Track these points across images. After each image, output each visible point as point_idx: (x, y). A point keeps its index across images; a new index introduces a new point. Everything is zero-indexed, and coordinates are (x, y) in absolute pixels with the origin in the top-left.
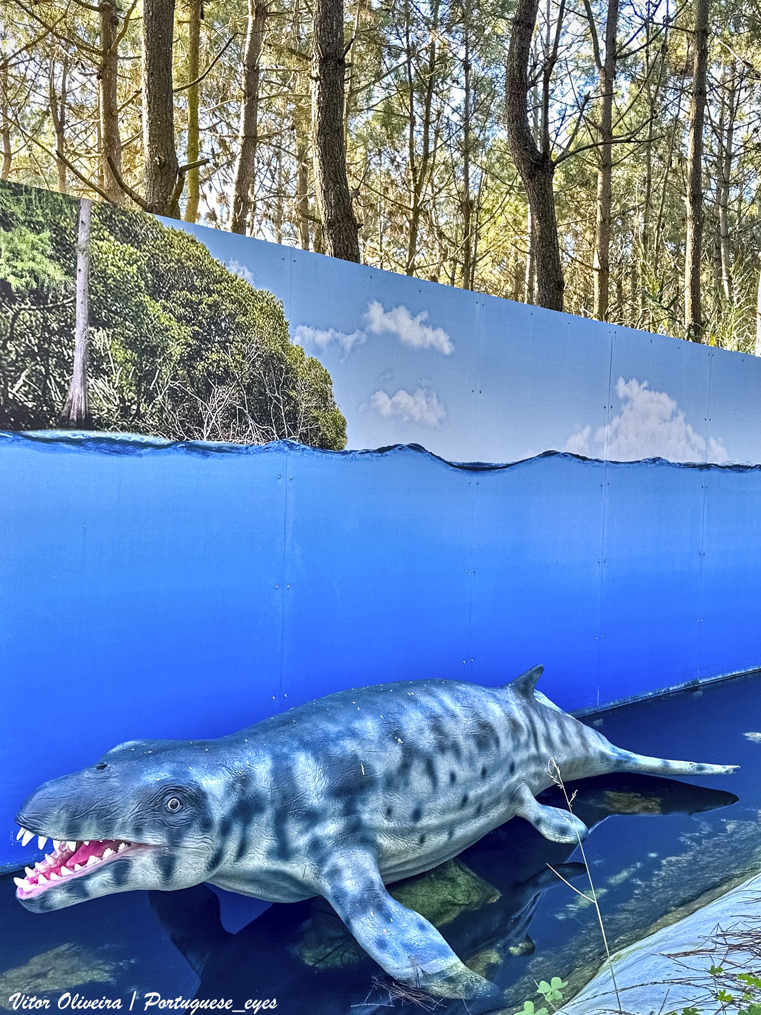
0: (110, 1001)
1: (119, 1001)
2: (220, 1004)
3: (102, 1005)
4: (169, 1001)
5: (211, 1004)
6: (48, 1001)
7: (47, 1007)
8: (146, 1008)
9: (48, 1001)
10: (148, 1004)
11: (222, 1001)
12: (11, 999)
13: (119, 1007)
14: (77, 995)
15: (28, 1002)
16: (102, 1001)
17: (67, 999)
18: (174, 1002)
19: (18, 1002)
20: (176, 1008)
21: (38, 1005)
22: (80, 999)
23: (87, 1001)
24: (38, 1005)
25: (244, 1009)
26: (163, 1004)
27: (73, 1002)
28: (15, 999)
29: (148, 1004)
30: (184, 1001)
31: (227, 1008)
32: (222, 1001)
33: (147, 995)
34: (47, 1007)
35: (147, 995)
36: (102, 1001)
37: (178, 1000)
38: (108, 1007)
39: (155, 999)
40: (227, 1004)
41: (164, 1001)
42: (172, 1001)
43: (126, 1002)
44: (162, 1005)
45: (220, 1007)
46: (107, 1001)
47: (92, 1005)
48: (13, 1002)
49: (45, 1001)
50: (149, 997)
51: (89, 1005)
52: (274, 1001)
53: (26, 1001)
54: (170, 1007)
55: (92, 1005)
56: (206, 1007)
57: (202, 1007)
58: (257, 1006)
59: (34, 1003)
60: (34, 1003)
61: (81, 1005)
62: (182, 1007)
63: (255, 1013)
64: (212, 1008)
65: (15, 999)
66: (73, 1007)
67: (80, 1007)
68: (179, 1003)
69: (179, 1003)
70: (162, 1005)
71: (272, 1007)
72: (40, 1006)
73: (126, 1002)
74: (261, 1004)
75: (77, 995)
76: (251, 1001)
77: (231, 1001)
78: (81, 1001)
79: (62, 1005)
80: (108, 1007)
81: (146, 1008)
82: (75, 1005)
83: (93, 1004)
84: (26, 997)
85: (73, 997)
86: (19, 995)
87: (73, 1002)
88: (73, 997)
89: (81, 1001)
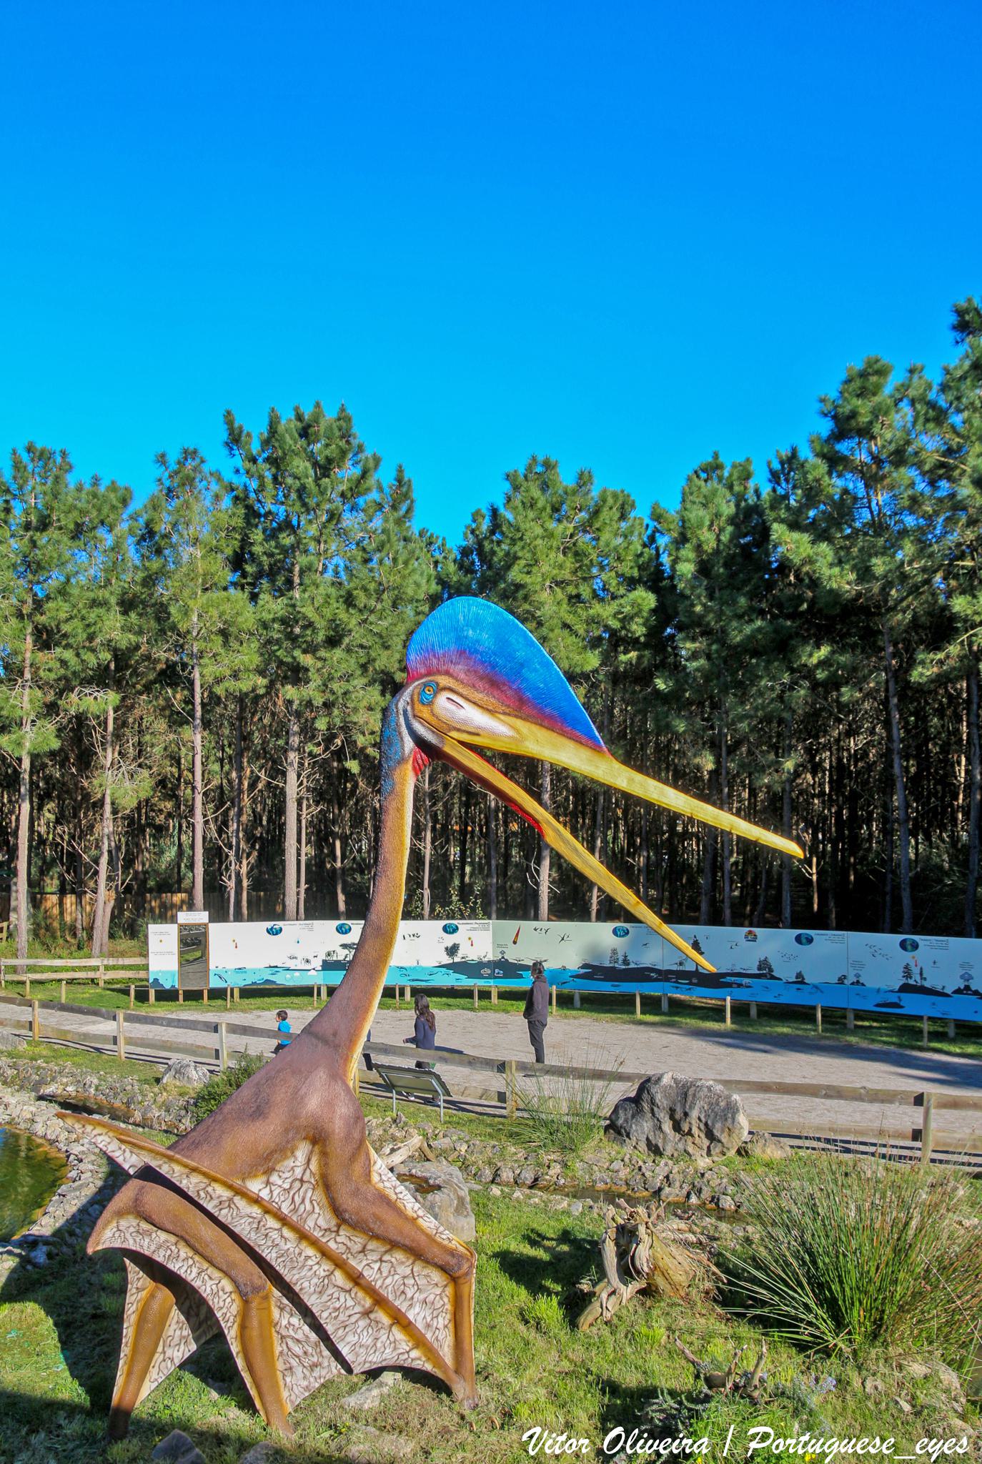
0: (690, 1441)
4: (789, 1441)
14: (636, 1431)
15: (555, 1442)
17: (619, 1436)
18: (797, 1444)
19: (535, 1445)
23: (651, 1442)
26: (778, 1446)
27: (629, 1443)
28: (531, 1437)
29: (753, 1445)
31: (886, 1452)
32: (878, 1440)
33: (752, 1431)
38: (688, 1451)
39: (765, 1437)
40: (885, 1445)
41: (781, 1440)
42: (793, 1441)
44: (777, 1447)
45: (873, 1451)
48: (528, 1443)
50: (754, 1437)
51: (655, 1447)
53: (550, 1442)
56: (850, 1451)
57: (843, 1451)
65: (531, 1437)
68: (806, 1444)
69: (806, 1444)
70: (777, 1447)
78: (642, 1441)
83: (662, 1446)
86: (538, 1430)
87: (629, 1443)
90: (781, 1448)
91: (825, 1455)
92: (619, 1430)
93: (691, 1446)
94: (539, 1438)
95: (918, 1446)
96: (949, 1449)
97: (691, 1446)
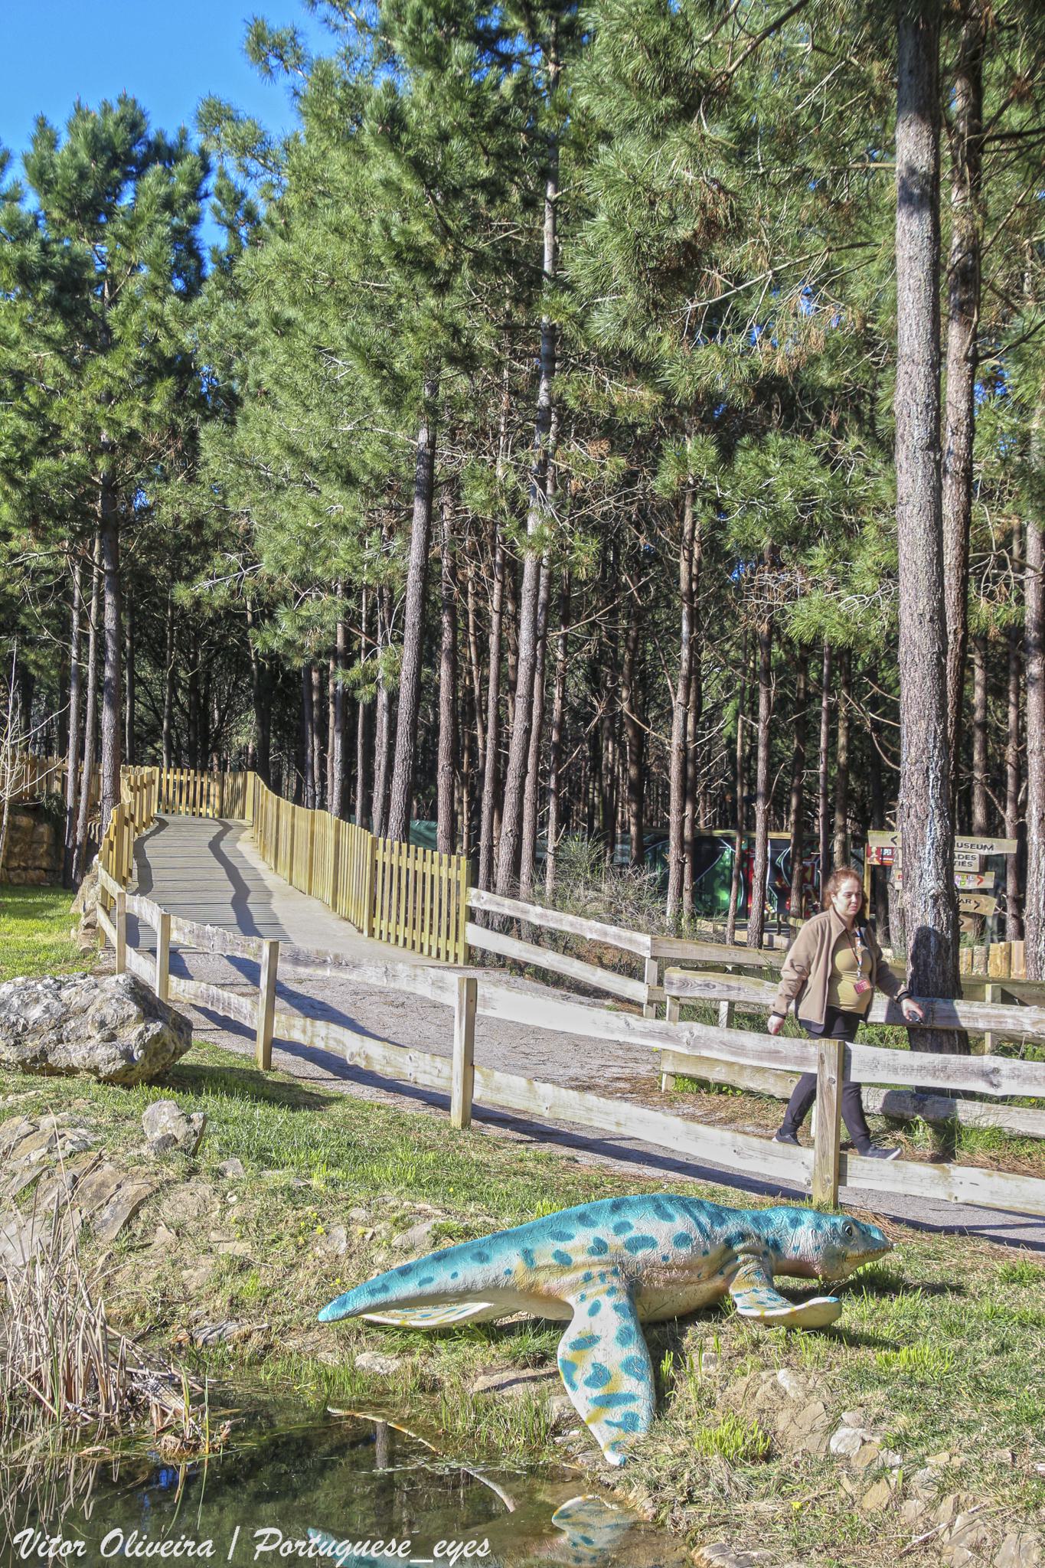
0: (193, 1544)
1: (210, 1542)
2: (389, 1549)
3: (179, 1550)
5: (373, 1548)
6: (82, 1544)
7: (80, 1554)
8: (256, 1557)
9: (82, 1544)
10: (261, 1548)
11: (393, 1543)
12: (16, 1540)
13: (209, 1554)
14: (136, 1533)
16: (179, 1544)
17: (116, 1539)
18: (308, 1545)
20: (311, 1555)
22: (139, 1539)
23: (151, 1544)
25: (432, 1556)
26: (287, 1548)
27: (128, 1546)
29: (261, 1548)
32: (393, 1543)
33: (259, 1533)
34: (80, 1554)
35: (259, 1533)
36: (179, 1544)
39: (273, 1538)
40: (400, 1548)
41: (289, 1543)
42: (303, 1544)
43: (221, 1547)
44: (285, 1550)
46: (187, 1544)
47: (162, 1550)
48: (18, 1546)
49: (77, 1543)
50: (262, 1537)
51: (155, 1550)
52: (486, 1543)
53: (43, 1544)
55: (162, 1550)
58: (455, 1550)
60: (57, 1548)
61: (141, 1550)
63: (338, 1565)
67: (139, 1555)
68: (316, 1548)
70: (285, 1550)
71: (481, 1554)
72: (69, 1551)
73: (221, 1547)
74: (369, 1548)
75: (136, 1533)
76: (445, 1542)
77: (409, 1543)
78: (141, 1544)
79: (107, 1551)
80: (190, 1554)
81: (256, 1557)
82: (132, 1549)
84: (43, 1536)
85: (126, 1534)
87: (128, 1546)
88: (126, 1534)
89: (141, 1544)
90: (289, 1551)
91: (335, 1557)
92: (117, 1532)
94: (32, 1540)
95: (436, 1549)
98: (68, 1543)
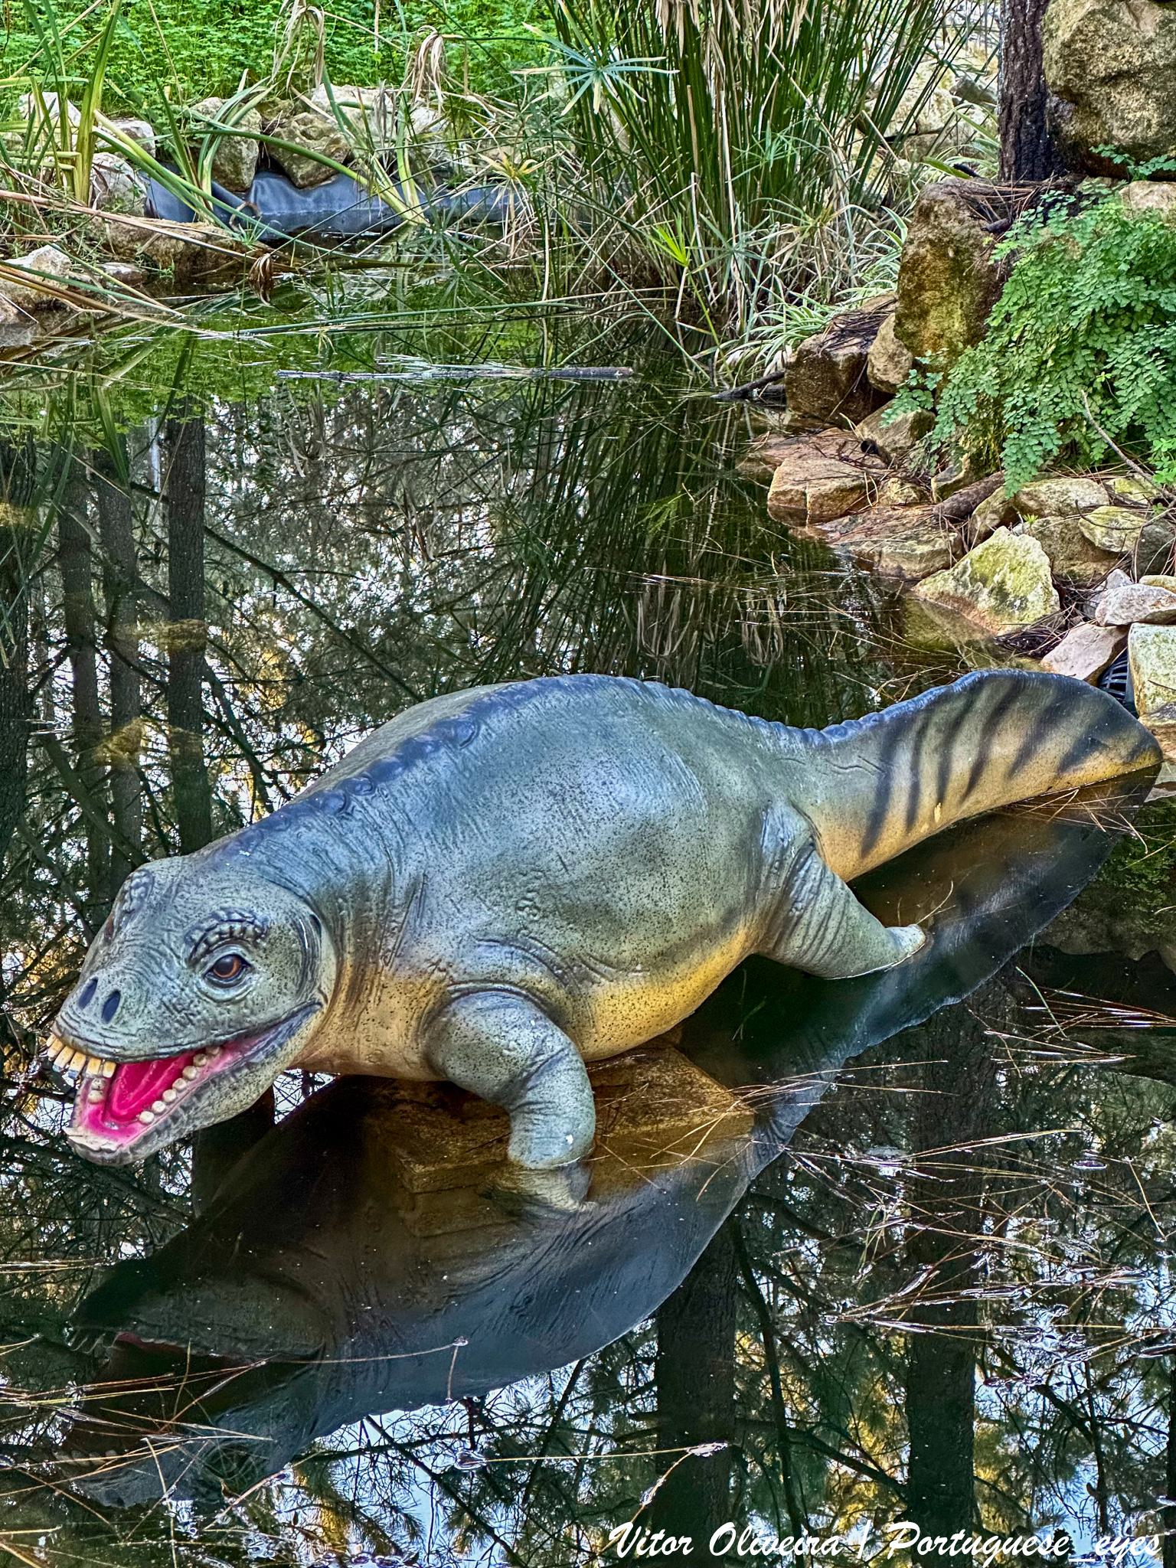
4: (938, 1540)
7: (686, 1552)
9: (688, 1540)
17: (726, 1537)
18: (950, 1542)
20: (953, 1553)
21: (668, 1548)
24: (668, 1548)
27: (741, 1542)
30: (969, 1540)
34: (686, 1552)
37: (957, 1537)
40: (1057, 1546)
41: (928, 1539)
42: (944, 1540)
44: (924, 1548)
49: (682, 1540)
53: (643, 1540)
54: (941, 1552)
56: (1015, 1552)
57: (1006, 1552)
59: (660, 1543)
60: (660, 1543)
62: (965, 1552)
64: (1027, 1553)
66: (741, 1553)
68: (960, 1543)
69: (960, 1543)
72: (673, 1549)
79: (718, 1547)
82: (744, 1547)
87: (741, 1542)
90: (929, 1549)
92: (728, 1527)
93: (819, 1545)
96: (1029, 1550)
97: (819, 1545)
98: (672, 1539)
